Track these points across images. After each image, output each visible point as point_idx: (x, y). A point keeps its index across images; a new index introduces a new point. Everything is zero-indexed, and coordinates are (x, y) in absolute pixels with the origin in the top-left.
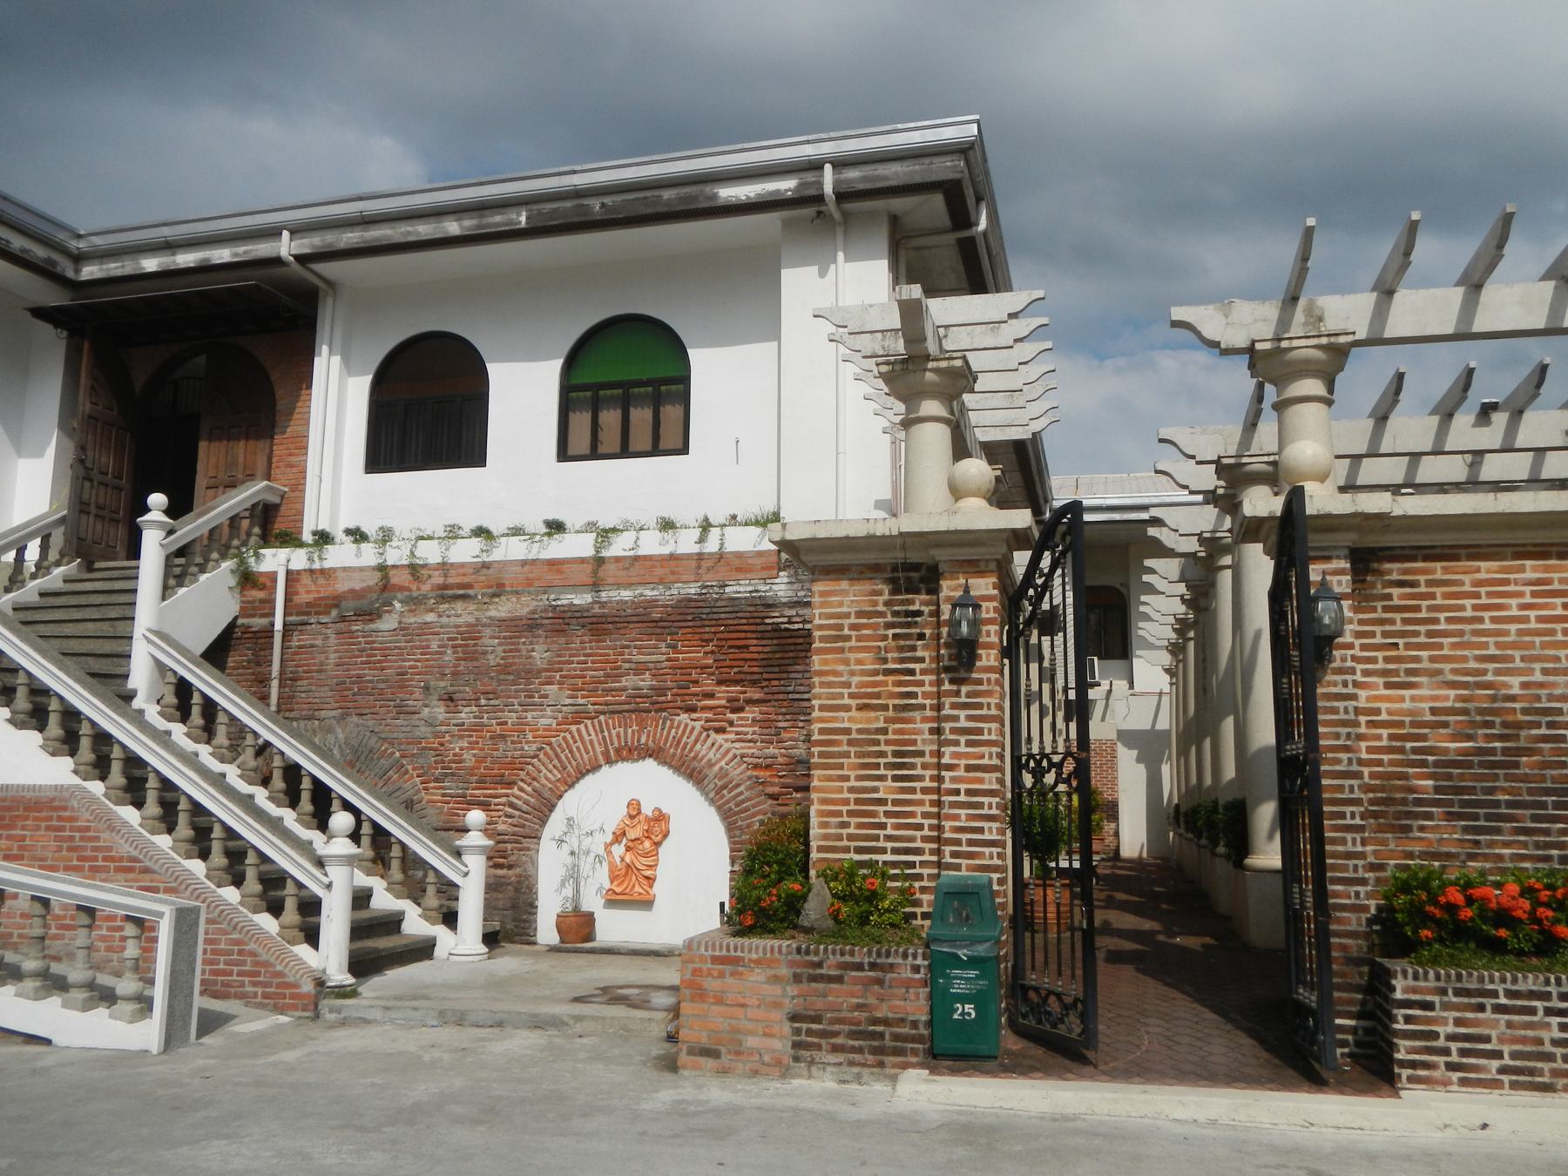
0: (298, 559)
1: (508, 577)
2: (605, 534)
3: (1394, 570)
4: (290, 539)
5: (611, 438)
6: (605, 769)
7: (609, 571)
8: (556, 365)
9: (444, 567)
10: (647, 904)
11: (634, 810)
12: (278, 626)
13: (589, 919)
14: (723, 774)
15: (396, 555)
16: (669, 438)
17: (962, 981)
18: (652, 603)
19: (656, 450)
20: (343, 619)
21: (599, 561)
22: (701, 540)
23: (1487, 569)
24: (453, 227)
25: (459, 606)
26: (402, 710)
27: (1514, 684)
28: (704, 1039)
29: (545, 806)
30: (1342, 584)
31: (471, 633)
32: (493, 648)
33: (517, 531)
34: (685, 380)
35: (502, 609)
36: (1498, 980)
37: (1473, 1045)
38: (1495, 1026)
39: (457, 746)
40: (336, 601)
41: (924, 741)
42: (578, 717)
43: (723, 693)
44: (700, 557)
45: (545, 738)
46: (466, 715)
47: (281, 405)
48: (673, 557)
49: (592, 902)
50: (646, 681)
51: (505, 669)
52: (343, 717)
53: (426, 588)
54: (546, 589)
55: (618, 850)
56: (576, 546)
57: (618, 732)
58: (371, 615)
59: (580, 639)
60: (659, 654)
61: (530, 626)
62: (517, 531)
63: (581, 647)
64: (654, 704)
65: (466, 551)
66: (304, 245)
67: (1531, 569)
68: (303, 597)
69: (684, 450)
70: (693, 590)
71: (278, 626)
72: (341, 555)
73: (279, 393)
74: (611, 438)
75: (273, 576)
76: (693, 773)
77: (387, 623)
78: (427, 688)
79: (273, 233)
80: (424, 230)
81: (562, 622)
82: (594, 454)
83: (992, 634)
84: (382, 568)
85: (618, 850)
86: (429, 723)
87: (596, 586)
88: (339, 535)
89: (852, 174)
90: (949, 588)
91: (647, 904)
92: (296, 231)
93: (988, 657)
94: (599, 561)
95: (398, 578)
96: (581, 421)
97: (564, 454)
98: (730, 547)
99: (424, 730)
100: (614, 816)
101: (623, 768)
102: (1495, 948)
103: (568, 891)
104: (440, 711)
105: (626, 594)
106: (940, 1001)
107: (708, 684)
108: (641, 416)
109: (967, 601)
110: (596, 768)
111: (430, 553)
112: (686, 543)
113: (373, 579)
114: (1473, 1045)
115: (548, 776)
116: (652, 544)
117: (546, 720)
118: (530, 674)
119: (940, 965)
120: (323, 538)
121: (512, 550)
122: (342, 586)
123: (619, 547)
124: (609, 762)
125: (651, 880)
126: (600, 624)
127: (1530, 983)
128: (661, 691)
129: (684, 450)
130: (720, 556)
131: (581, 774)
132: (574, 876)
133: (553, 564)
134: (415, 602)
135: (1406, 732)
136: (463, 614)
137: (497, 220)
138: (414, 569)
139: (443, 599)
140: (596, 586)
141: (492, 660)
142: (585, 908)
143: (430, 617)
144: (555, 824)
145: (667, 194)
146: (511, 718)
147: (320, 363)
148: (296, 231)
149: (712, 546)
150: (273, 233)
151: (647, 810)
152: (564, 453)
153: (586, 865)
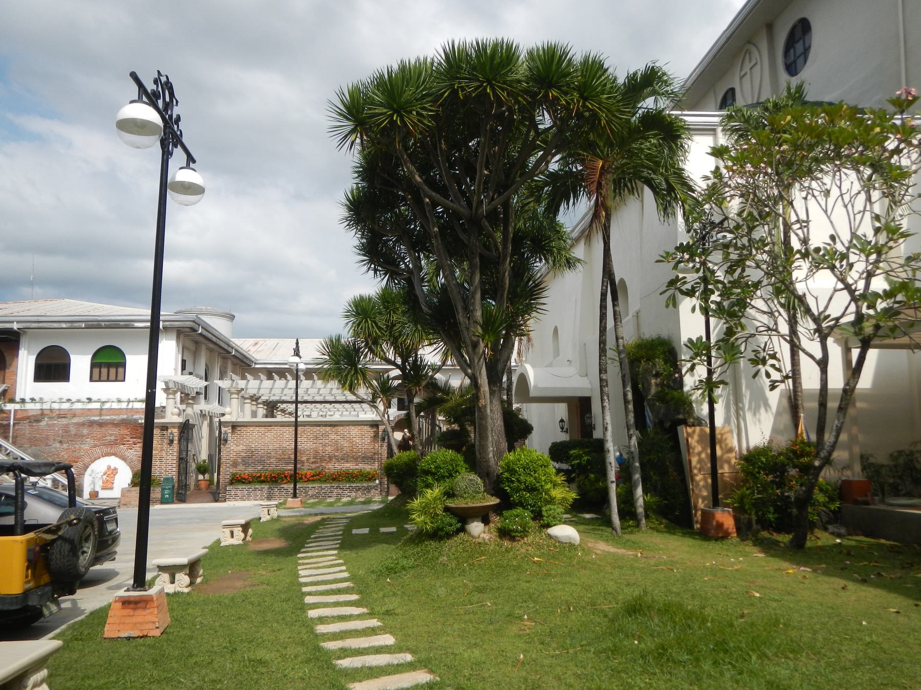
0: (17, 407)
1: (77, 413)
2: (104, 403)
3: (239, 429)
4: (12, 401)
5: (104, 376)
6: (102, 459)
7: (104, 412)
8: (90, 357)
9: (59, 410)
10: (112, 488)
11: (109, 468)
12: (12, 423)
13: (97, 492)
14: (131, 459)
15: (46, 406)
16: (120, 377)
17: (166, 492)
18: (115, 419)
19: (116, 380)
20: (30, 422)
21: (102, 409)
22: (128, 405)
23: (251, 428)
24: (64, 325)
25: (63, 419)
26: (47, 445)
27: (253, 446)
28: (124, 503)
29: (86, 467)
30: (230, 431)
31: (67, 425)
32: (73, 430)
33: (79, 401)
34: (124, 365)
35: (75, 420)
36: (240, 487)
37: (236, 495)
38: (239, 493)
39: (63, 454)
40: (28, 418)
41: (164, 455)
42: (95, 446)
43: (132, 441)
44: (127, 409)
45: (86, 451)
46: (65, 446)
47: (8, 362)
48: (120, 409)
49: (98, 489)
50: (113, 438)
51: (76, 435)
52: (30, 447)
53: (54, 415)
54: (87, 416)
55: (105, 477)
56: (97, 406)
57: (105, 450)
58: (38, 421)
59: (96, 428)
60: (116, 431)
61: (83, 424)
62: (79, 401)
63: (96, 431)
64: (115, 443)
65: (66, 406)
66: (21, 326)
67: (257, 429)
68: (18, 416)
69: (124, 380)
70: (125, 417)
71: (12, 423)
72: (29, 406)
73: (7, 359)
74: (104, 376)
75: (10, 411)
76: (124, 458)
77: (43, 423)
78: (54, 440)
79: (12, 322)
80: (56, 325)
81: (92, 424)
82: (100, 380)
83: (176, 438)
84: (42, 410)
85: (105, 477)
86: (55, 448)
87: (101, 415)
88: (28, 400)
89: (167, 323)
90: (169, 431)
91: (112, 488)
92: (18, 322)
93: (176, 442)
94: (102, 409)
95: (45, 412)
96: (96, 371)
97: (91, 380)
98: (135, 407)
99: (53, 450)
100: (103, 468)
101: (107, 458)
102: (244, 483)
103: (92, 486)
104: (58, 445)
105: (108, 417)
106: (163, 495)
107: (128, 438)
108: (113, 371)
109: (171, 433)
110: (99, 458)
111: (56, 406)
112: (124, 405)
113: (39, 412)
114: (236, 495)
115: (87, 460)
116: (115, 406)
117: (86, 447)
118: (83, 436)
119: (163, 490)
120: (23, 401)
121: (78, 406)
122: (30, 414)
123: (107, 406)
124: (103, 456)
125: (113, 483)
126: (101, 424)
127: (244, 487)
128: (116, 440)
129: (124, 380)
130: (132, 409)
131: (96, 459)
132: (94, 483)
133: (89, 409)
134: (51, 418)
135: (238, 453)
136: (64, 421)
137: (76, 325)
138: (51, 410)
139: (59, 418)
140: (101, 415)
141: (73, 433)
142: (96, 490)
143: (55, 422)
144: (89, 471)
145: (122, 323)
146: (77, 446)
147: (20, 352)
148: (18, 322)
149: (130, 406)
150: (12, 322)
151: (112, 467)
152: (91, 380)
153: (96, 481)
